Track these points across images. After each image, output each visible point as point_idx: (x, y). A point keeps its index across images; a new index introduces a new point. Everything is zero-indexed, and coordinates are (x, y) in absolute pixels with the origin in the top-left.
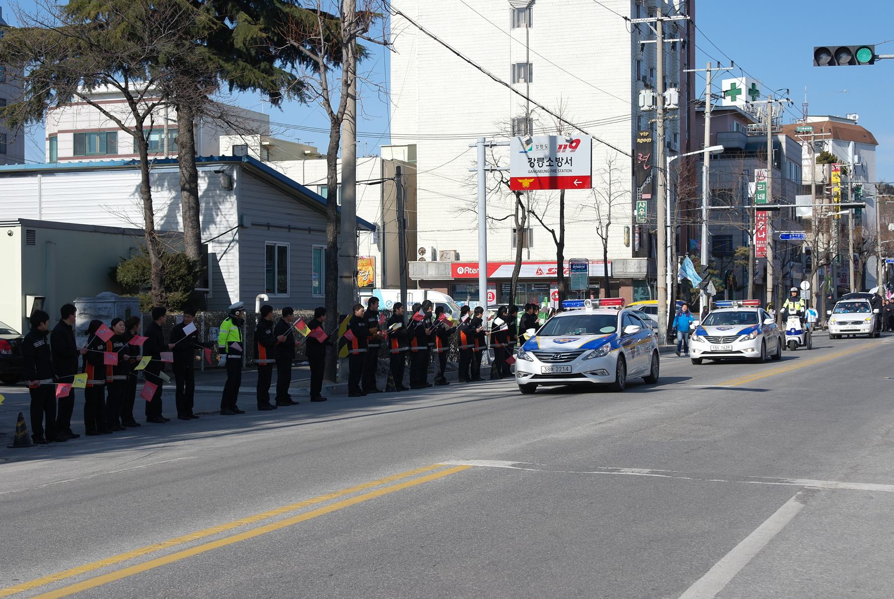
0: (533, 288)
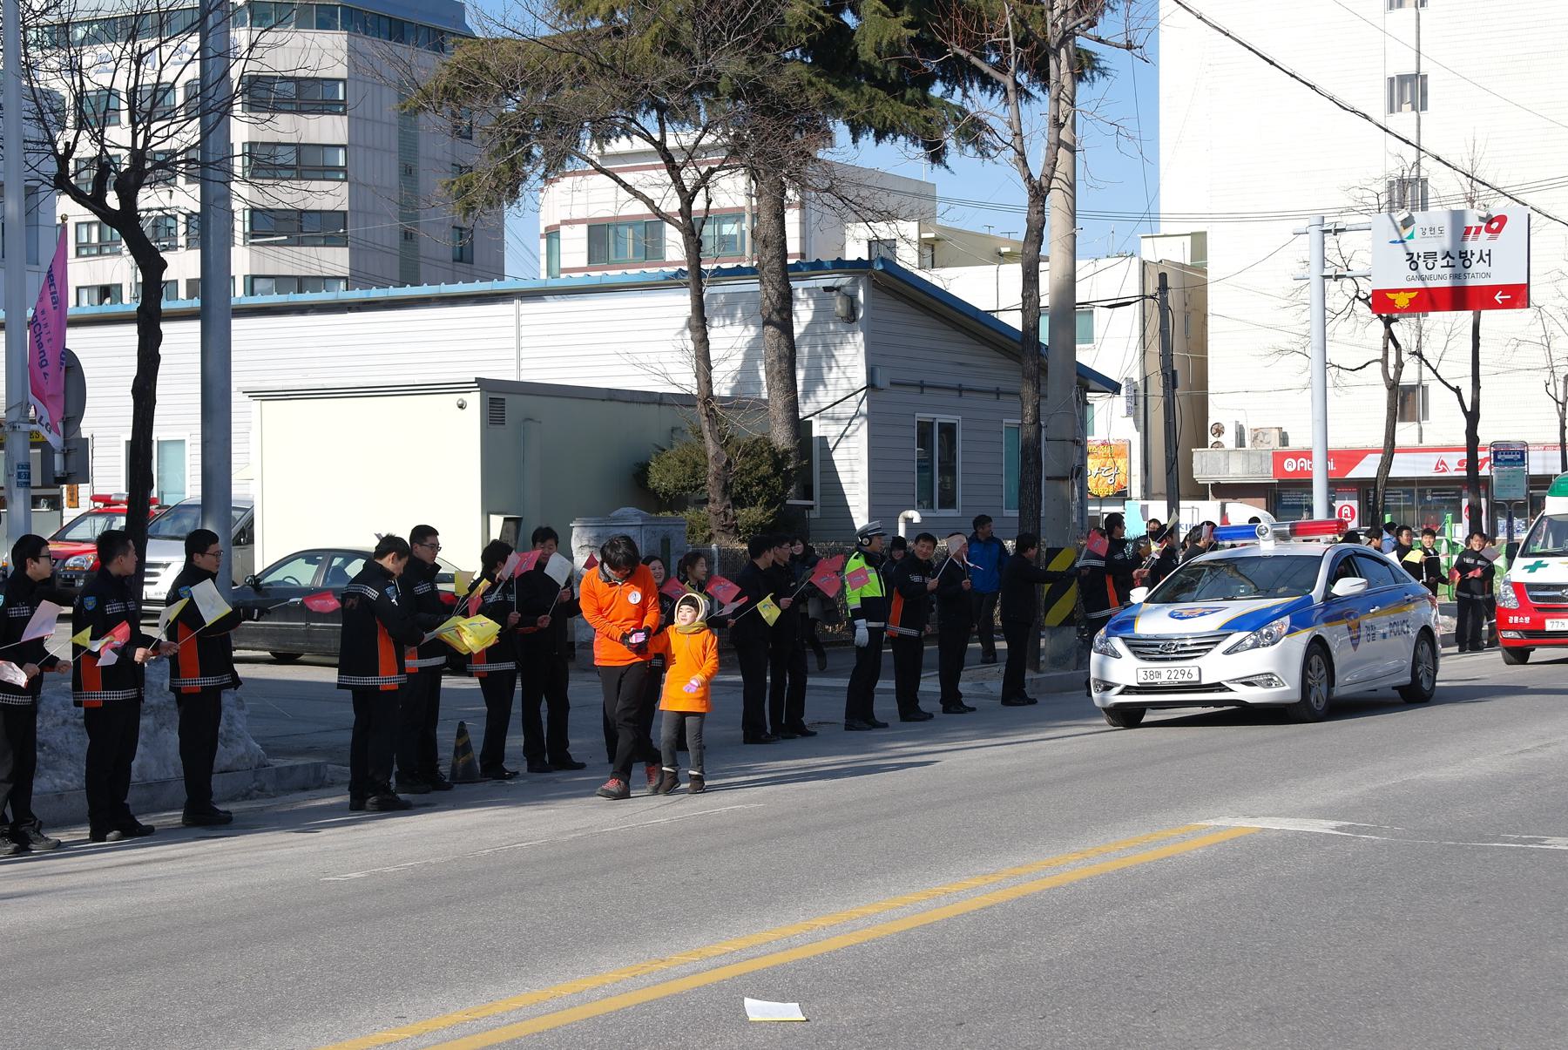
0: (1429, 498)
